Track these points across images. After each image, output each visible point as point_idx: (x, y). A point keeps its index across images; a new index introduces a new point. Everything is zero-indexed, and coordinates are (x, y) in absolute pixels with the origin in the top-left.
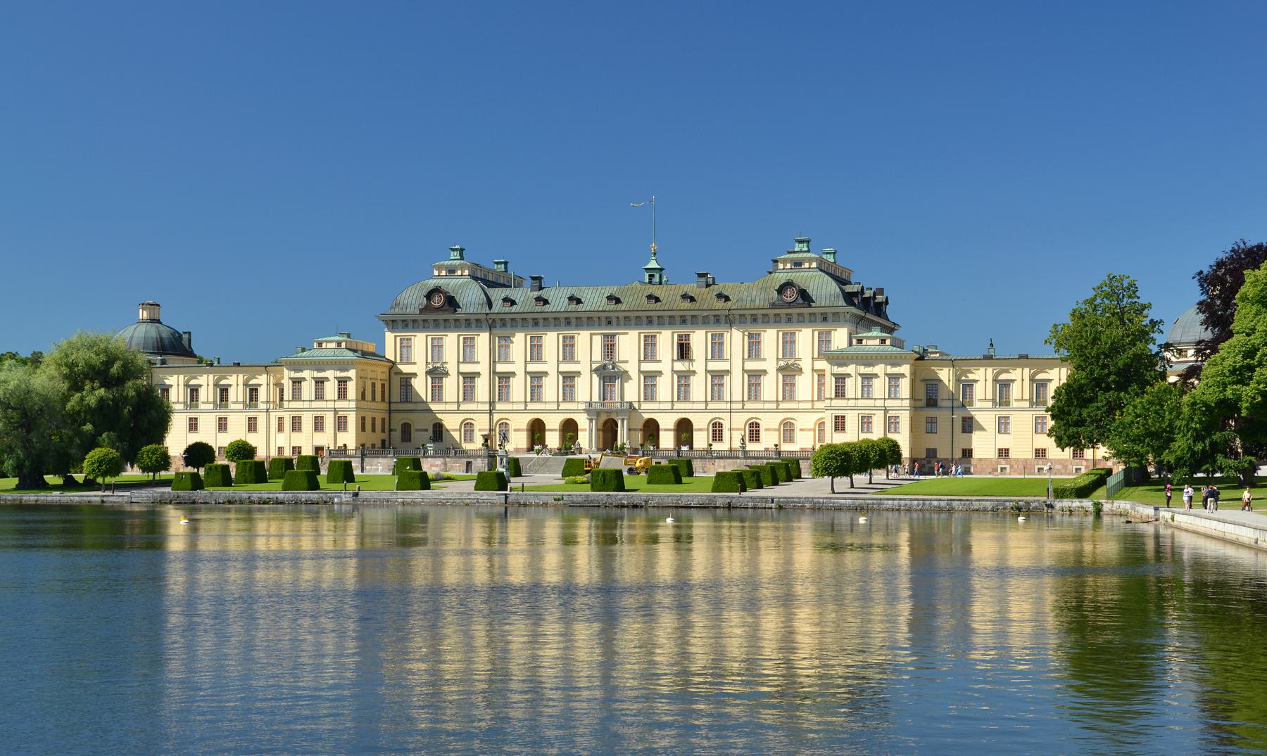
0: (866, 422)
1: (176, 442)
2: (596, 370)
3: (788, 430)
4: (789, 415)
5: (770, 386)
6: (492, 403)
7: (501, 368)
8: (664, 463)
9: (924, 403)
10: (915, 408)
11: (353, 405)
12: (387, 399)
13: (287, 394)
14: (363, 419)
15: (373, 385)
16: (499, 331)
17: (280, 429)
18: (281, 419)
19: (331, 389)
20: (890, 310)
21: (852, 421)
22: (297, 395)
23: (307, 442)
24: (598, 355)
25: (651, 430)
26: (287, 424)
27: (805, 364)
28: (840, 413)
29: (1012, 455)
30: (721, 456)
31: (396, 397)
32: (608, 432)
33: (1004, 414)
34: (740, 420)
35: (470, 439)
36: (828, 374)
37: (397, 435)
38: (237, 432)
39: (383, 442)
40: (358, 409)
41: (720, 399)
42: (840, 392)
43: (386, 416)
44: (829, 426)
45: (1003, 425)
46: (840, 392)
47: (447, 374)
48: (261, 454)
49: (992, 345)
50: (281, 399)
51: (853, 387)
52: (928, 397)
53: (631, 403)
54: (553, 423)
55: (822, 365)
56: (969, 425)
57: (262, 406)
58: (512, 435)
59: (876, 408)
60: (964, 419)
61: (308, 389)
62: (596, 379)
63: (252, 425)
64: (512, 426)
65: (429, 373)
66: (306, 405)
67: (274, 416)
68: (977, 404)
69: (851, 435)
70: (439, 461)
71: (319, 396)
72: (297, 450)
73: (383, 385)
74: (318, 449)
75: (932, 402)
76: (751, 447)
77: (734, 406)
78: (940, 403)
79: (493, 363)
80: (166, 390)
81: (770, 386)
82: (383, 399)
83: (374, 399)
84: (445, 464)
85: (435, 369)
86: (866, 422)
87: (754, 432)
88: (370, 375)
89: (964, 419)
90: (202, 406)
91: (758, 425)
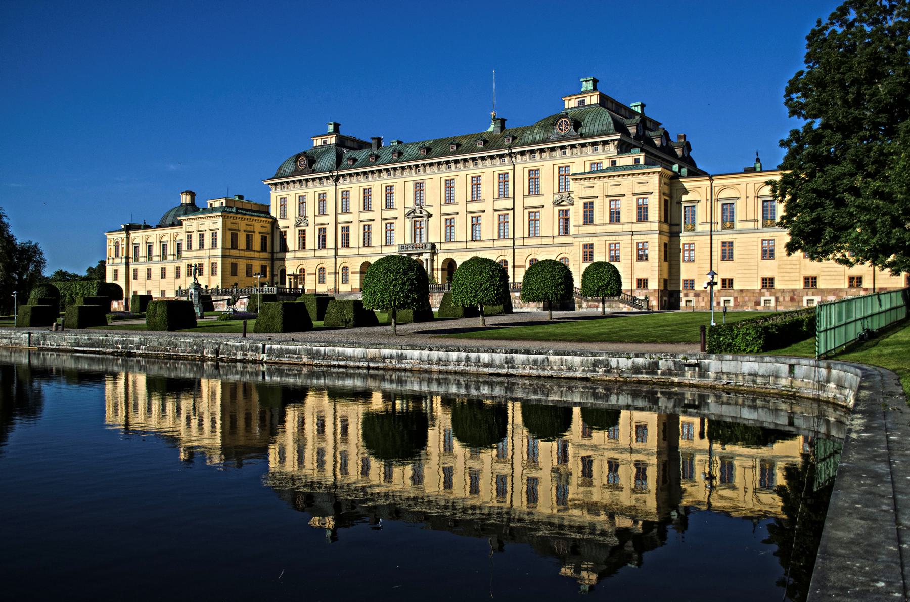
4: (564, 249)
6: (336, 249)
12: (269, 248)
16: (342, 186)
18: (178, 269)
24: (410, 203)
28: (588, 241)
31: (277, 248)
42: (588, 220)
46: (588, 220)
49: (758, 160)
53: (433, 246)
56: (728, 252)
58: (350, 275)
59: (623, 233)
60: (724, 244)
64: (350, 271)
65: (298, 225)
68: (738, 226)
73: (264, 239)
78: (699, 228)
79: (336, 214)
82: (264, 248)
83: (249, 247)
89: (724, 244)
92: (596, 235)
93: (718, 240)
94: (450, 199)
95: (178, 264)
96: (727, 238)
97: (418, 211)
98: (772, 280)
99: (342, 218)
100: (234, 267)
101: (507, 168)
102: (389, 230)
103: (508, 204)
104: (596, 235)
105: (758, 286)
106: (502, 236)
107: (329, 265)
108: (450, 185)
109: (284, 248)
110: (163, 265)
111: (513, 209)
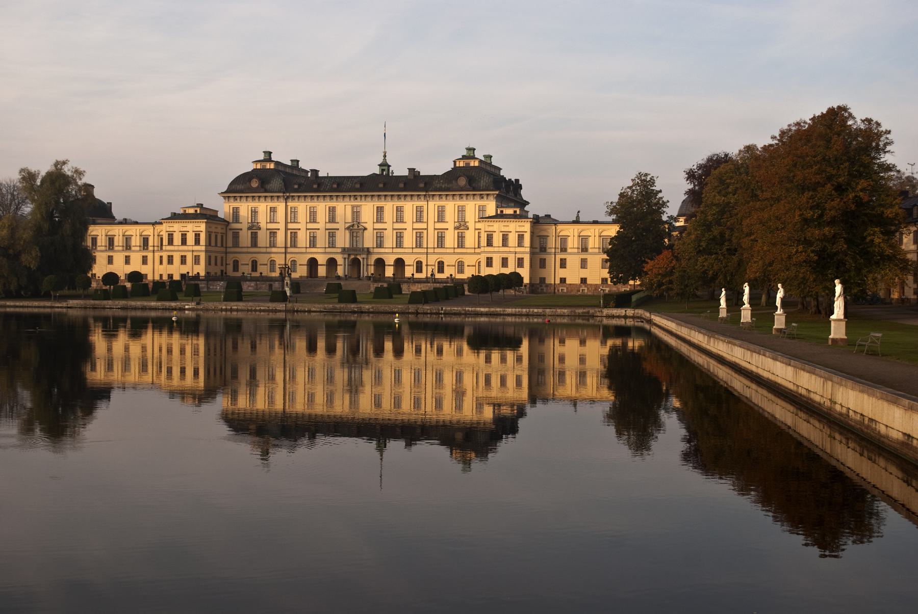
0: (505, 262)
1: (100, 269)
2: (348, 228)
3: (461, 267)
5: (451, 239)
6: (286, 248)
7: (290, 226)
8: (385, 285)
9: (538, 250)
10: (532, 254)
11: (203, 248)
13: (165, 242)
14: (210, 257)
15: (216, 236)
16: (290, 204)
17: (161, 263)
18: (161, 257)
19: (191, 239)
20: (525, 194)
21: (497, 262)
22: (171, 242)
23: (177, 271)
24: (349, 219)
25: (380, 263)
26: (165, 260)
27: (471, 225)
28: (489, 255)
29: (589, 282)
30: (420, 281)
31: (230, 244)
32: (355, 264)
33: (584, 256)
34: (433, 260)
35: (272, 269)
36: (482, 232)
37: (230, 268)
38: (136, 265)
39: (222, 271)
40: (206, 251)
41: (421, 247)
43: (224, 255)
44: (483, 263)
45: (584, 264)
47: (260, 229)
48: (150, 278)
50: (162, 245)
51: (497, 240)
52: (539, 248)
54: (322, 259)
55: (479, 225)
56: (563, 264)
57: (151, 248)
58: (298, 267)
60: (561, 260)
61: (177, 239)
62: (347, 232)
63: (145, 260)
64: (298, 264)
65: (249, 228)
66: (176, 248)
67: (157, 255)
68: (569, 250)
69: (496, 270)
70: (253, 284)
71: (184, 242)
72: (170, 276)
74: (183, 276)
75: (543, 249)
76: (438, 276)
77: (429, 251)
79: (286, 223)
80: (94, 240)
81: (451, 239)
82: (222, 246)
83: (216, 245)
84: (257, 285)
85: (253, 226)
86: (505, 262)
87: (441, 267)
88: (213, 230)
89: (561, 260)
90: (116, 248)
91: (443, 263)
92: (494, 252)
93: (559, 257)
94: (380, 218)
95: (145, 254)
96: (563, 256)
97: (356, 227)
98: (586, 279)
99: (290, 226)
100: (210, 257)
101: (422, 203)
102: (332, 235)
103: (424, 226)
104: (494, 252)
105: (578, 282)
106: (419, 245)
107: (280, 260)
108: (380, 210)
109: (236, 243)
110: (127, 254)
111: (427, 229)
